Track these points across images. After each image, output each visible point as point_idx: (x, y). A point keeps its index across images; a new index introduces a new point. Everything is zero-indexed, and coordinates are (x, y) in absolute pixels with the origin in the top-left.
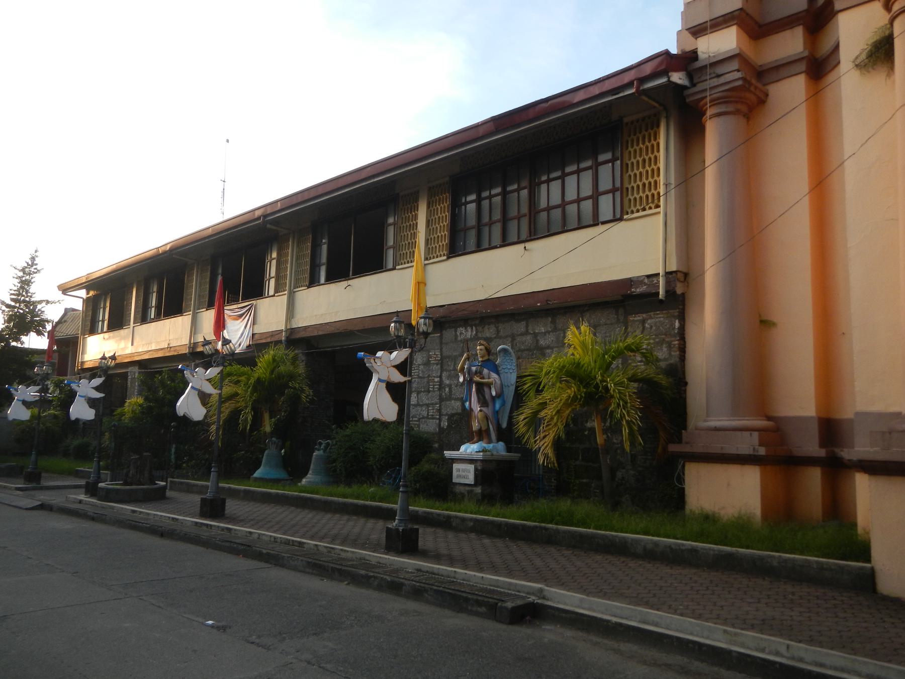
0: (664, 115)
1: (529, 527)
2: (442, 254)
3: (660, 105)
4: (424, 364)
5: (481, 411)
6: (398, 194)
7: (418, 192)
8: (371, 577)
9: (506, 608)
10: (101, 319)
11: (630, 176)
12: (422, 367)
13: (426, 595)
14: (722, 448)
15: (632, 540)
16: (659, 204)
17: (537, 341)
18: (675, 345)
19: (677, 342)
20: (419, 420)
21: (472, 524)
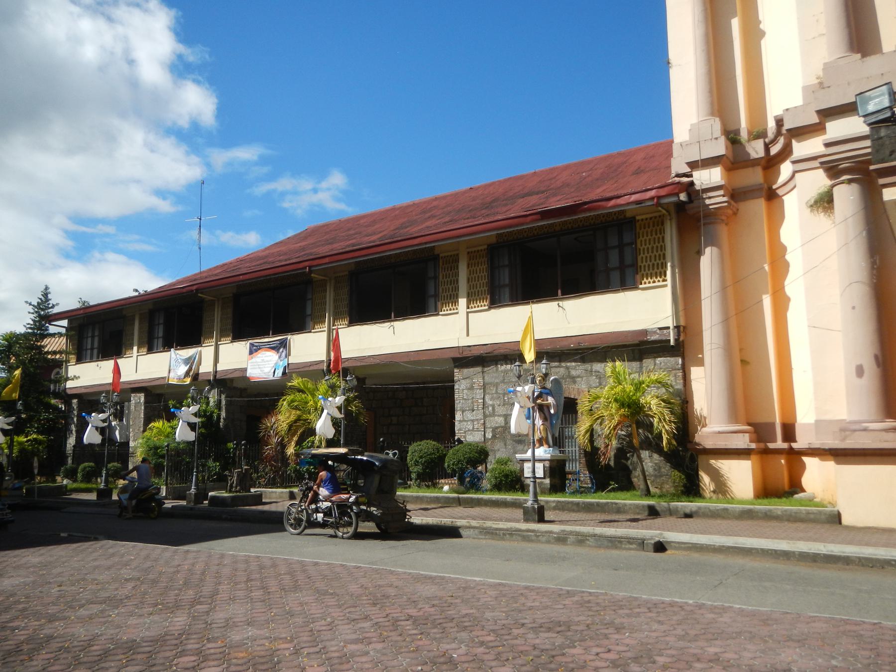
0: (669, 218)
1: (602, 503)
2: (480, 305)
3: (668, 211)
4: (469, 389)
5: (543, 424)
6: (438, 255)
7: (458, 255)
8: (540, 535)
9: (650, 543)
10: (89, 347)
11: (642, 258)
12: (465, 391)
13: (588, 542)
14: (726, 445)
15: (682, 506)
16: (666, 278)
17: (569, 372)
18: (679, 376)
19: (681, 374)
20: (465, 432)
21: (554, 504)
